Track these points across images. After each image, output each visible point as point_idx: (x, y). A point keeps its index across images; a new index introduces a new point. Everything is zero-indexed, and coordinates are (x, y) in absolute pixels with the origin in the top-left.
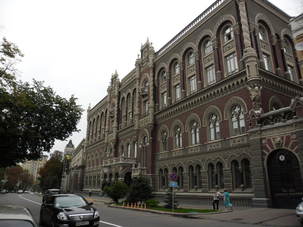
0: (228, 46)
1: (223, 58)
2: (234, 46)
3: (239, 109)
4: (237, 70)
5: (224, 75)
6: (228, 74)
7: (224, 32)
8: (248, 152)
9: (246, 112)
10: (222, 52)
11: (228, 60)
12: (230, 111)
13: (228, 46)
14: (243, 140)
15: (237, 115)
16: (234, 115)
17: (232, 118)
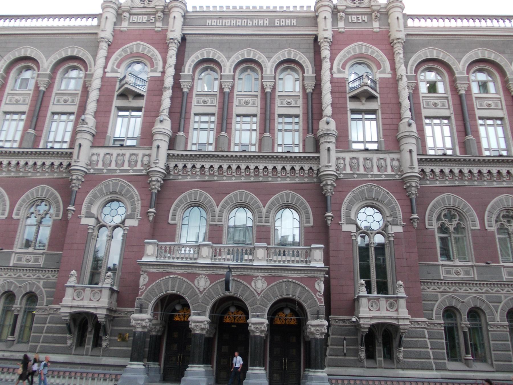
0: (65, 98)
1: (49, 114)
2: (76, 104)
3: (47, 208)
4: (66, 142)
5: (40, 141)
6: (47, 142)
7: (67, 71)
8: (39, 282)
10: (52, 102)
11: (56, 121)
12: (30, 204)
13: (65, 98)
14: (36, 260)
15: (40, 216)
16: (33, 215)
17: (28, 217)
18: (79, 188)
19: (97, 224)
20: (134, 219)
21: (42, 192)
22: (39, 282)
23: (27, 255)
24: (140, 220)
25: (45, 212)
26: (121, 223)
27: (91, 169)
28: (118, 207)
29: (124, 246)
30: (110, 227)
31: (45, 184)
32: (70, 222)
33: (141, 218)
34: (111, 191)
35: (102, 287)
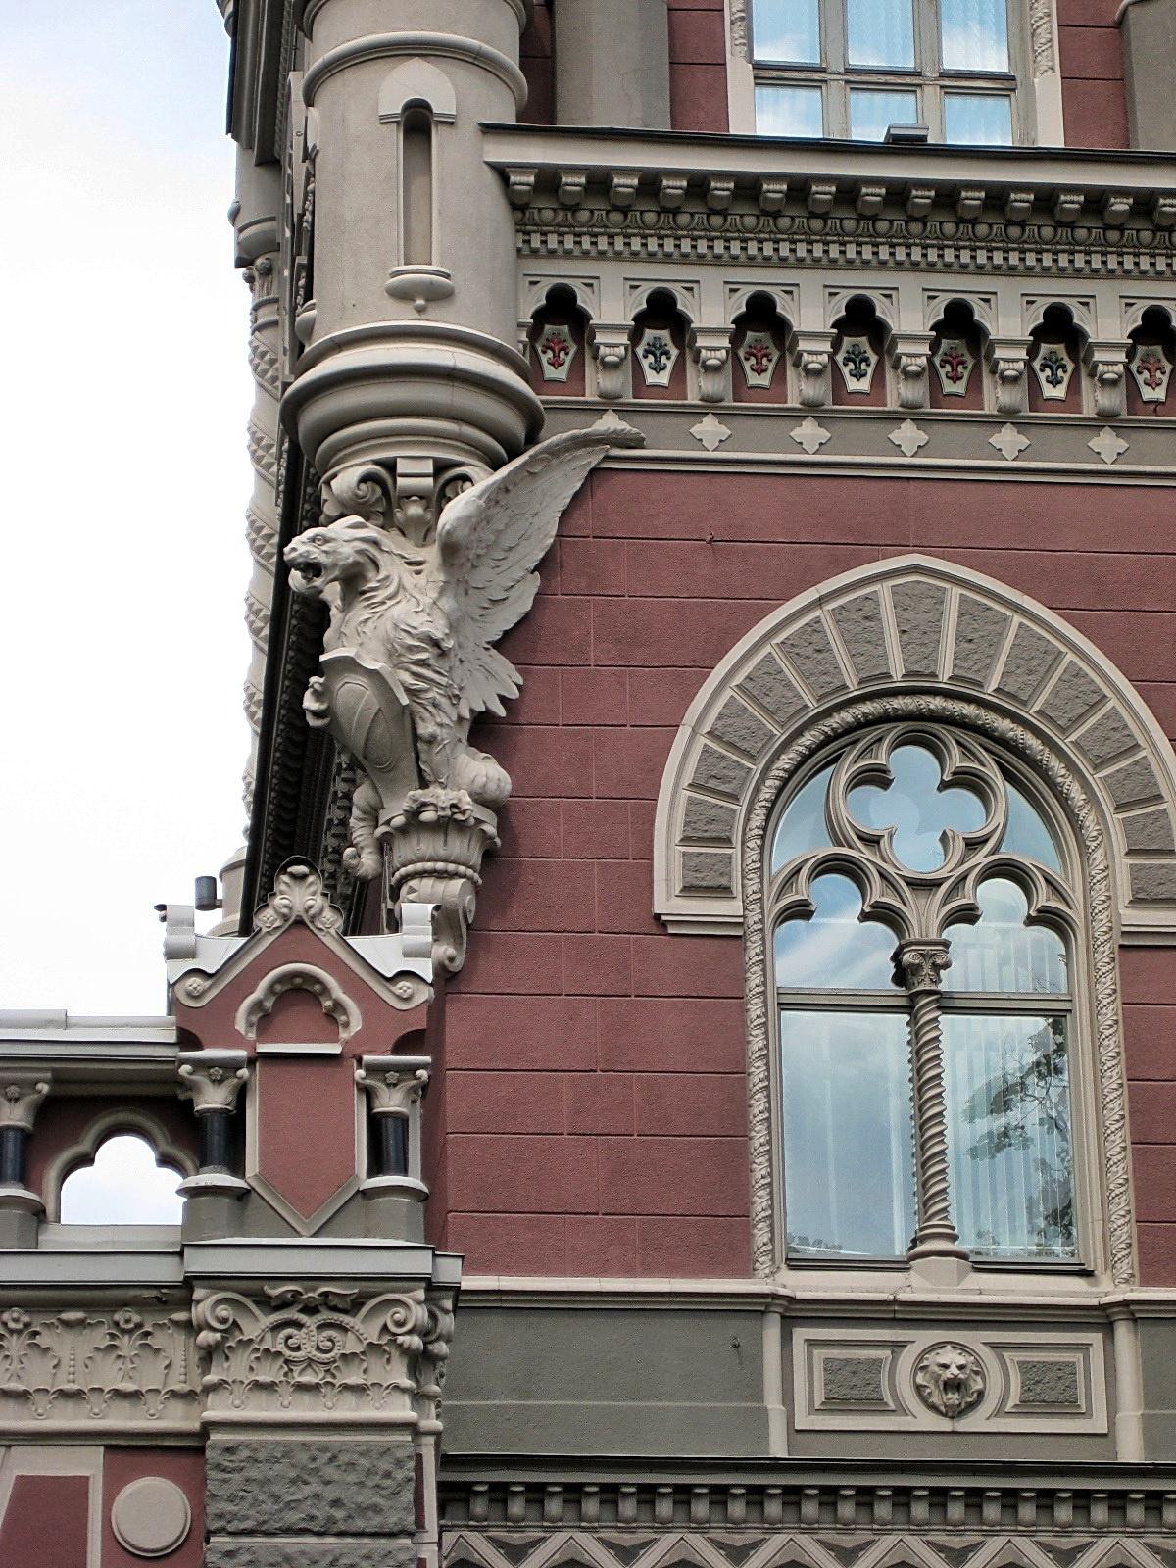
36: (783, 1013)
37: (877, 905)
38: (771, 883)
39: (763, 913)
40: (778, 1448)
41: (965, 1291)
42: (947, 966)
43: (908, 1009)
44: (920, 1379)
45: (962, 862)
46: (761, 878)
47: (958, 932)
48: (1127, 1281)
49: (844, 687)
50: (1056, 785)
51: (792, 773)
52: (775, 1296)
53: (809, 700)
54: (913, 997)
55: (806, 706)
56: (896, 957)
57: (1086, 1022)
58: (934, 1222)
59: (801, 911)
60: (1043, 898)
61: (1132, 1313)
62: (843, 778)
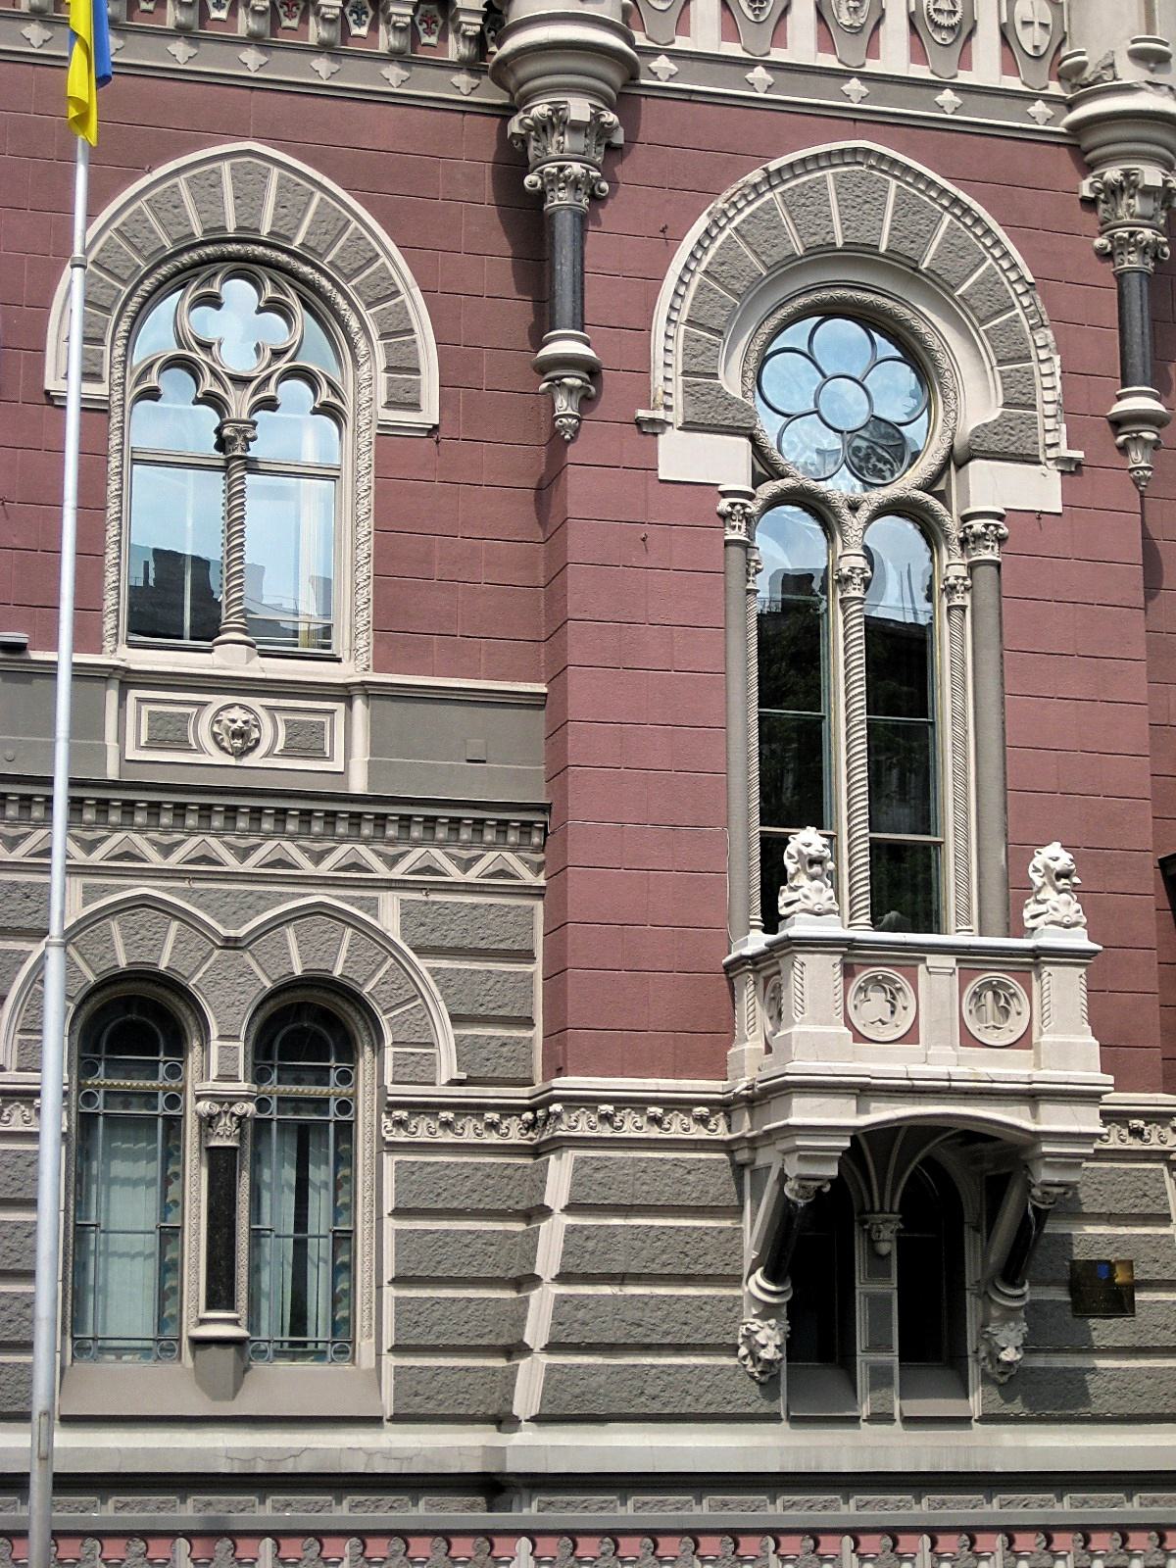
9: (415, 406)
18: (595, 198)
19: (757, 480)
20: (1031, 459)
21: (250, 200)
22: (372, 907)
23: (219, 700)
24: (1071, 469)
25: (283, 365)
26: (919, 488)
27: (653, 53)
28: (867, 361)
29: (990, 656)
30: (854, 507)
31: (257, 138)
32: (573, 453)
33: (1078, 454)
34: (840, 244)
35: (1036, 953)
36: (135, 467)
37: (207, 394)
38: (132, 373)
39: (124, 393)
40: (112, 773)
41: (249, 670)
42: (254, 439)
43: (224, 469)
44: (216, 729)
45: (269, 366)
46: (125, 368)
47: (261, 416)
48: (365, 670)
49: (193, 234)
50: (340, 315)
51: (151, 293)
52: (116, 668)
53: (168, 244)
54: (228, 461)
55: (164, 246)
56: (219, 431)
57: (349, 484)
58: (231, 620)
59: (153, 394)
60: (325, 394)
61: (366, 690)
62: (188, 301)
